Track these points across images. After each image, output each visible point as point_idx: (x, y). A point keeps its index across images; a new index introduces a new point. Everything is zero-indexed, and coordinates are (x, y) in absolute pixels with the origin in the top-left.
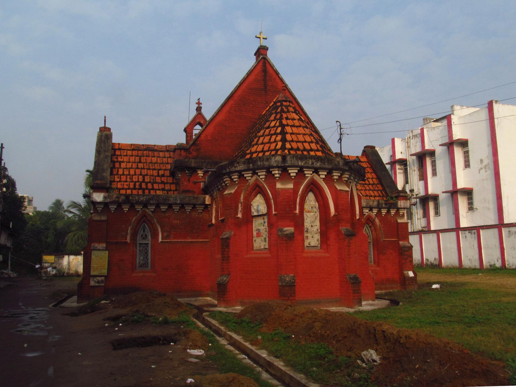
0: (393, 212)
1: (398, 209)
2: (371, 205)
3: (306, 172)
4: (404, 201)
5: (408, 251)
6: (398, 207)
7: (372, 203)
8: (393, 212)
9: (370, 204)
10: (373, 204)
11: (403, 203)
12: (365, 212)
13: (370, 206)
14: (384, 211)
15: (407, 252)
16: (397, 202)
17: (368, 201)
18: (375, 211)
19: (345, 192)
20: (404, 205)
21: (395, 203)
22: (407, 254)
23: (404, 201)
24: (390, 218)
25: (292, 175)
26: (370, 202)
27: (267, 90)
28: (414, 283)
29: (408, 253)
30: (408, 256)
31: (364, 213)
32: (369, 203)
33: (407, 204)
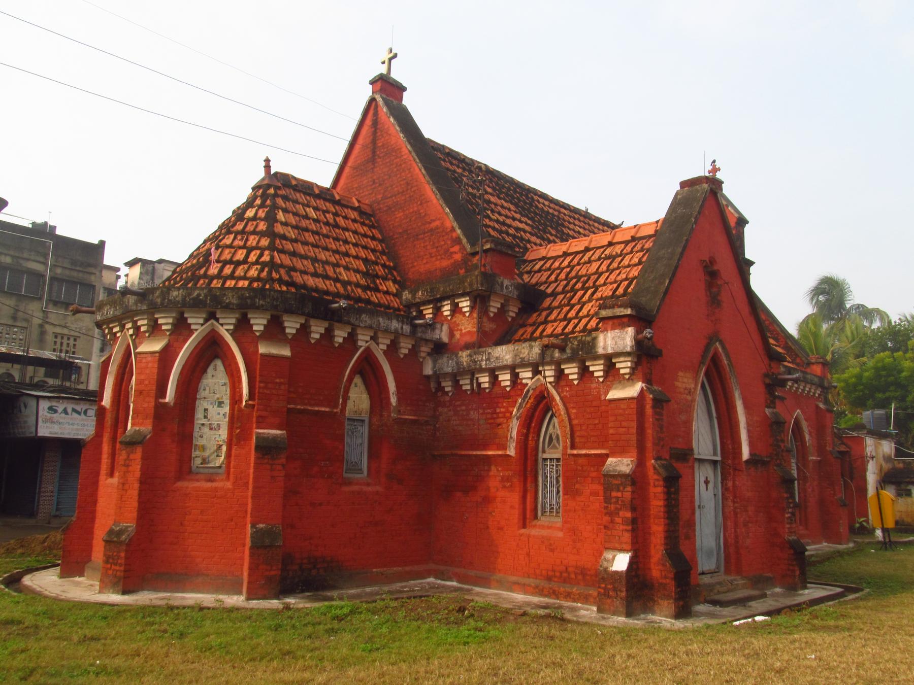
0: (597, 369)
1: (609, 362)
2: (524, 358)
3: (252, 322)
4: (616, 331)
5: (621, 488)
6: (596, 352)
7: (526, 353)
8: (597, 369)
9: (521, 356)
10: (528, 354)
11: (613, 338)
12: (525, 378)
13: (521, 362)
14: (572, 370)
15: (618, 491)
16: (595, 339)
17: (518, 349)
18: (549, 373)
19: (149, 355)
20: (616, 343)
21: (589, 342)
22: (617, 498)
23: (617, 332)
24: (596, 388)
25: (255, 328)
26: (523, 351)
27: (376, 157)
28: (621, 591)
29: (619, 494)
30: (620, 502)
31: (524, 381)
32: (521, 352)
33: (624, 339)
